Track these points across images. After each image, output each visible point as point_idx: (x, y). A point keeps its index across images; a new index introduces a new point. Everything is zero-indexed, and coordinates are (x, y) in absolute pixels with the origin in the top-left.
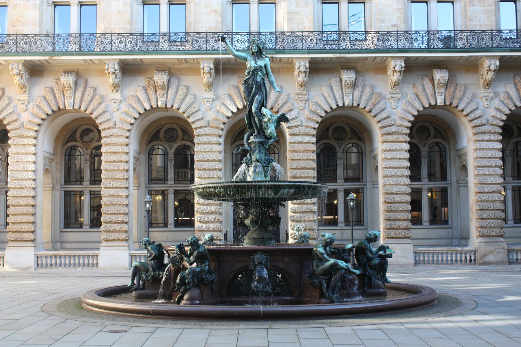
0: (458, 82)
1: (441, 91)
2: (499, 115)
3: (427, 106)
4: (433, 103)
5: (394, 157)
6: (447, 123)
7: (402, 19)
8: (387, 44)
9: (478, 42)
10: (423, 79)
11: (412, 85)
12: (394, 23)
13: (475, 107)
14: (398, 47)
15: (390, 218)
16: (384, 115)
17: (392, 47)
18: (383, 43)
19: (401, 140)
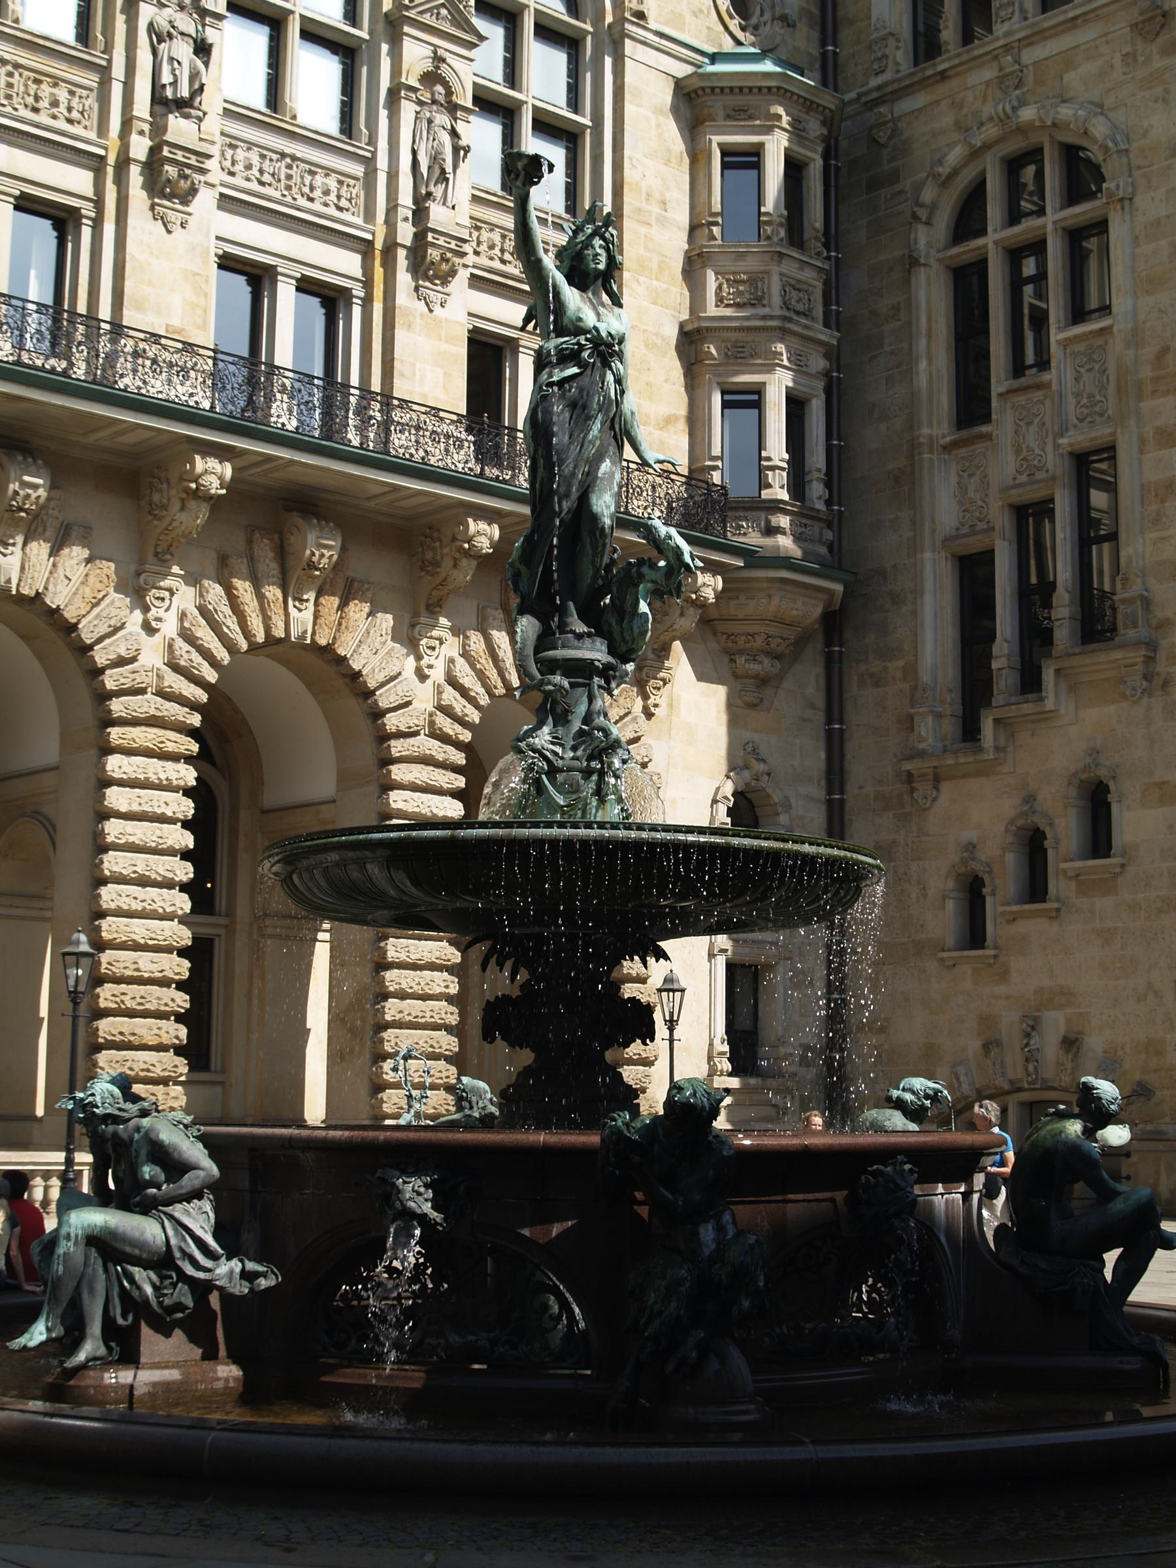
0: (351, 574)
1: (305, 597)
2: (460, 705)
3: (260, 638)
4: (279, 632)
5: (147, 808)
6: (237, 711)
7: (199, 312)
8: (179, 387)
9: (447, 451)
10: (250, 542)
11: (214, 555)
12: (176, 322)
13: (396, 670)
14: (213, 407)
15: (118, 1038)
16: (117, 647)
17: (196, 402)
18: (169, 382)
19: (170, 747)
